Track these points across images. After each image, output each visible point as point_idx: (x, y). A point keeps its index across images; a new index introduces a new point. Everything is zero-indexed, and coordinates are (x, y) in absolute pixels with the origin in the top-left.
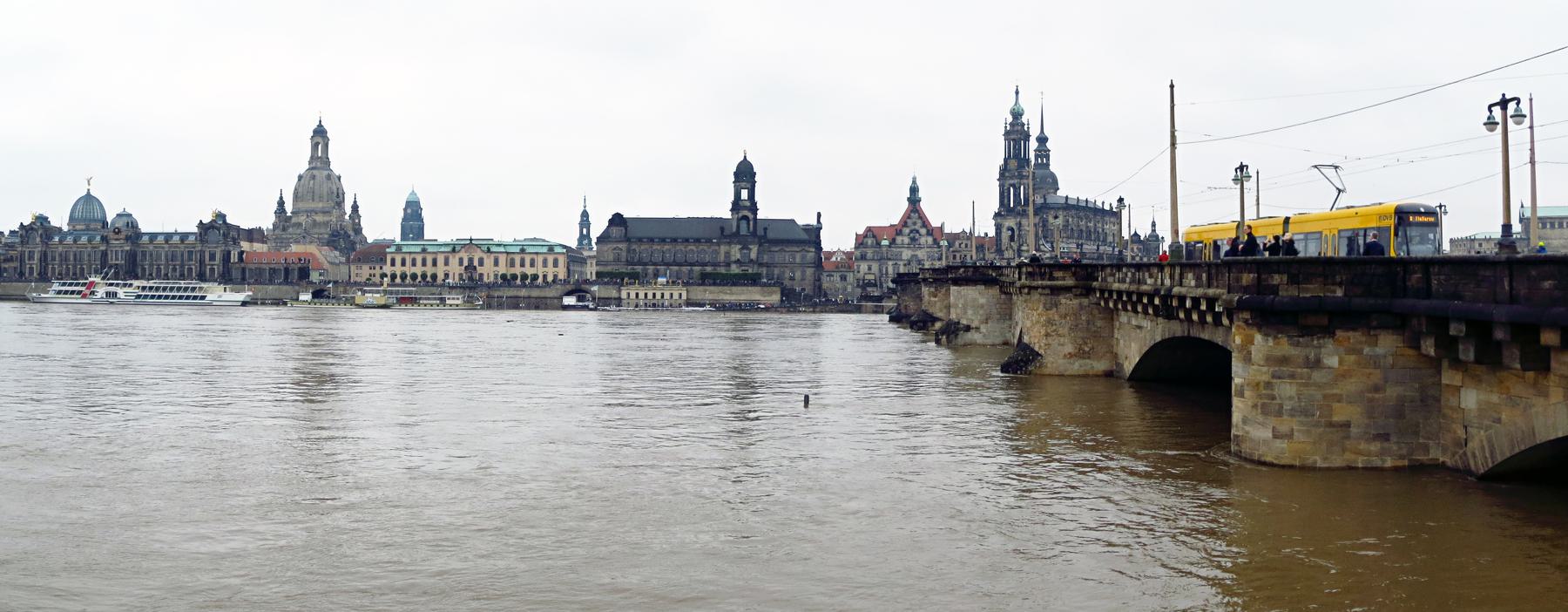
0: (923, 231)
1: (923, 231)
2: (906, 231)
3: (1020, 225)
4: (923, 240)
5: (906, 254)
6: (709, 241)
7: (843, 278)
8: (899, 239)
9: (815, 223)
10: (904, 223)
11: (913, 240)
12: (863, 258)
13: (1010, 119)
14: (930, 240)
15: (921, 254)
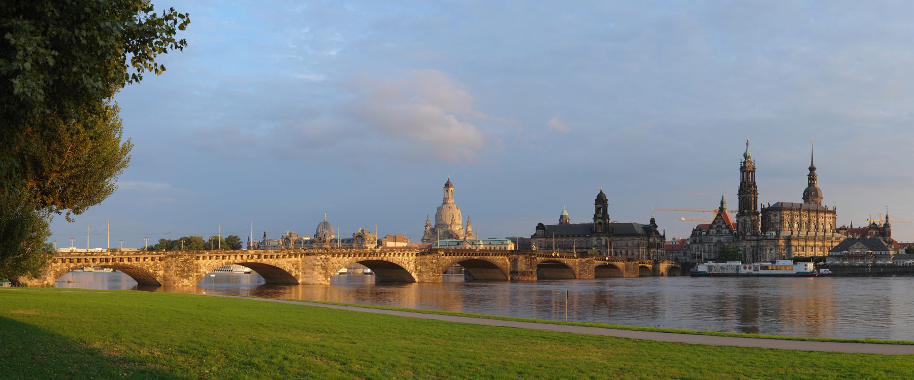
0: (724, 226)
1: (724, 226)
2: (715, 226)
3: (745, 220)
4: (723, 231)
5: (715, 239)
6: (585, 236)
7: (685, 254)
8: (711, 231)
9: (649, 223)
10: (714, 222)
11: (718, 231)
12: (694, 242)
13: (743, 160)
14: (727, 231)
15: (722, 239)
